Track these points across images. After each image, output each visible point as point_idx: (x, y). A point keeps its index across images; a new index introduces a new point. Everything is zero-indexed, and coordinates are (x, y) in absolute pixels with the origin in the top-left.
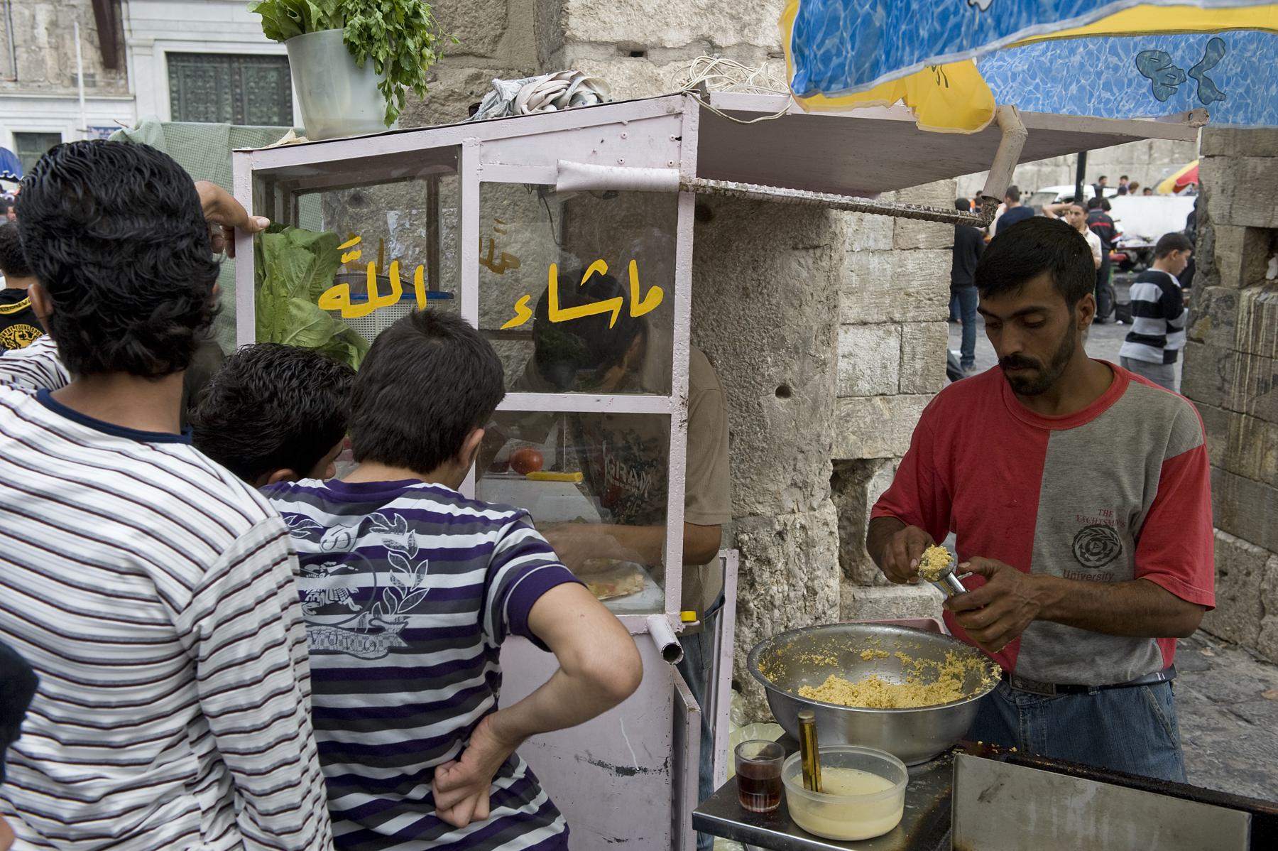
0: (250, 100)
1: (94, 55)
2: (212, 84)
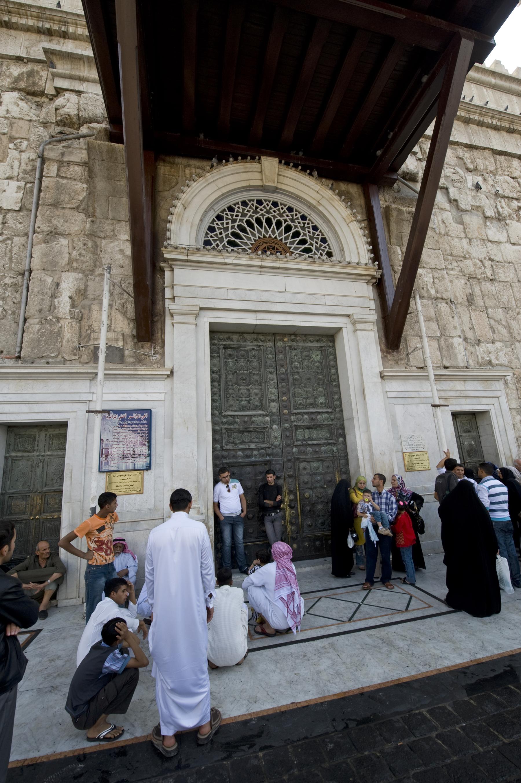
0: (294, 380)
1: (125, 326)
2: (255, 364)
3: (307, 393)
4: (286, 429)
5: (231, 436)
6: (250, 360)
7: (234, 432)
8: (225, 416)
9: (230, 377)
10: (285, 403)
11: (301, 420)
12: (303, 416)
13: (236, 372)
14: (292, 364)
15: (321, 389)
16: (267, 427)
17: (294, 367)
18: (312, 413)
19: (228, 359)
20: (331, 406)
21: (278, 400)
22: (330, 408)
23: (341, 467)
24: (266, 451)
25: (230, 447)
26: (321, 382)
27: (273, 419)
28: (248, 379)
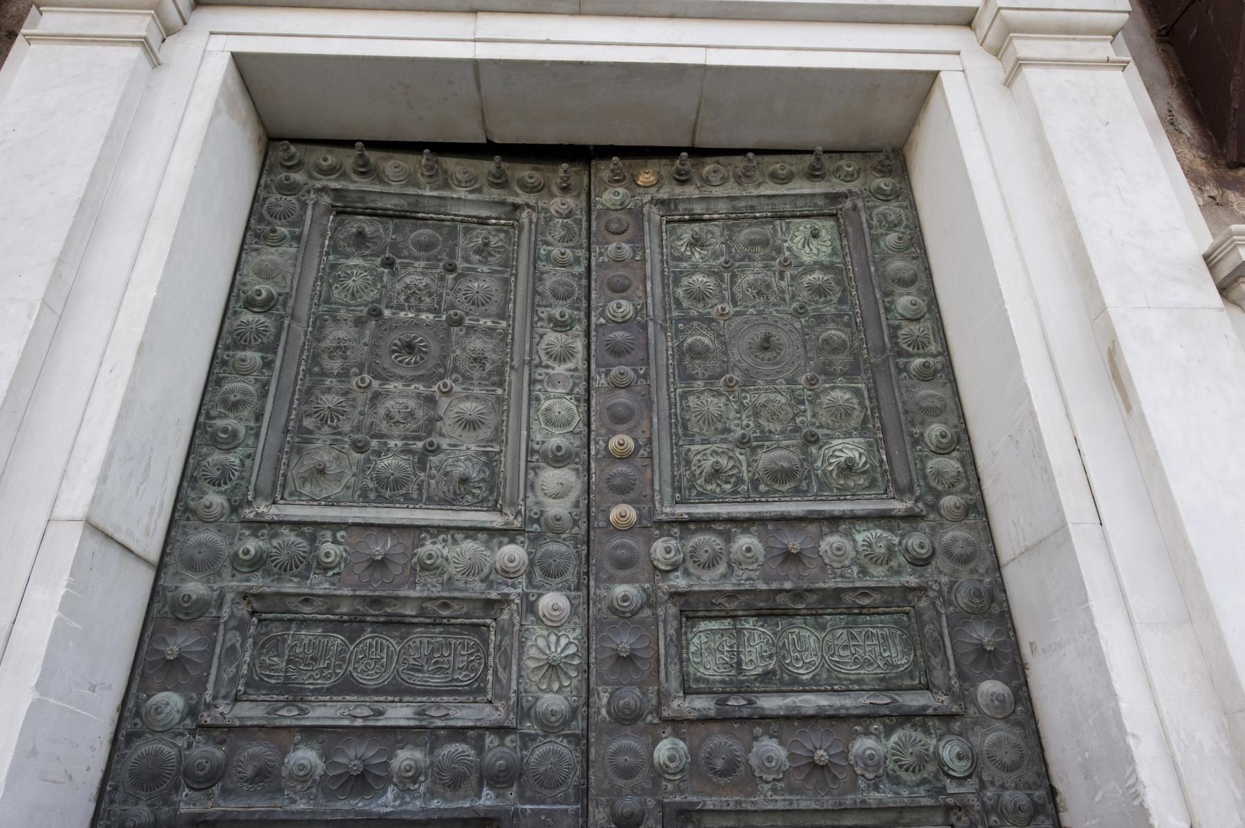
3: (756, 414)
4: (623, 615)
5: (276, 645)
6: (461, 265)
7: (304, 623)
8: (258, 526)
9: (339, 333)
10: (622, 468)
11: (711, 564)
12: (728, 538)
13: (376, 313)
14: (677, 282)
15: (840, 396)
16: (505, 601)
17: (690, 293)
18: (784, 520)
19: (347, 256)
20: (903, 481)
22: (901, 493)
24: (480, 749)
25: (251, 712)
26: (841, 361)
27: (549, 555)
28: (435, 348)
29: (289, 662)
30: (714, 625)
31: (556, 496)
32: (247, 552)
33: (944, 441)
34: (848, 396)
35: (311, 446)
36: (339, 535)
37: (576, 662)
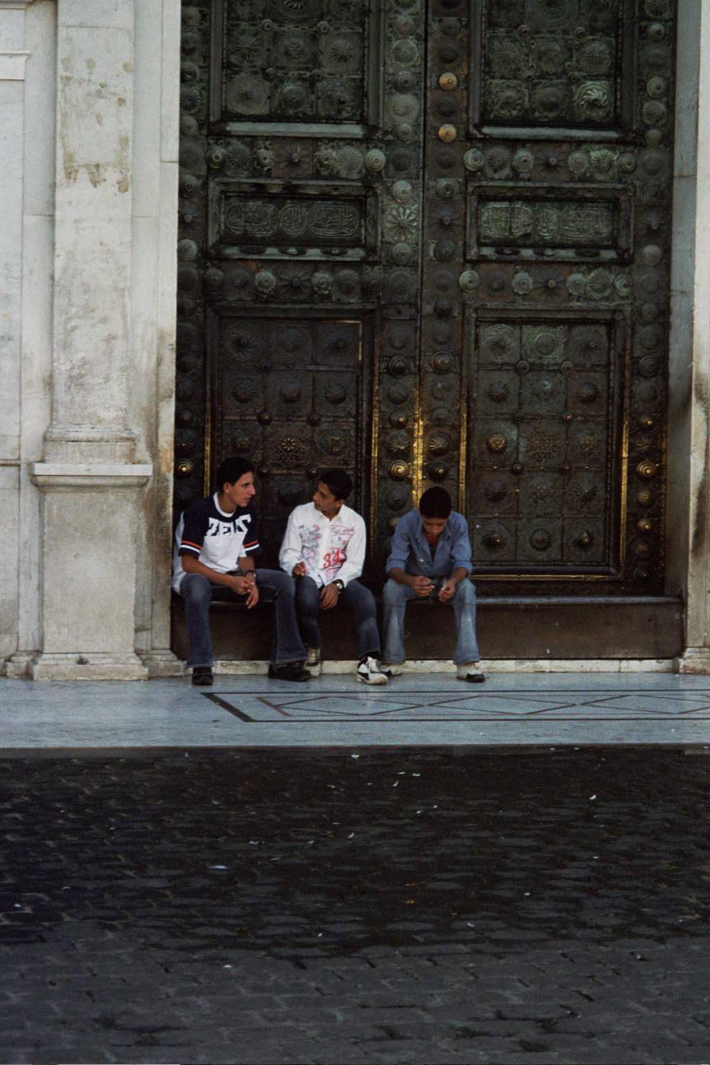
3: (540, 58)
4: (445, 198)
12: (514, 151)
18: (549, 141)
21: (421, 85)
23: (637, 353)
29: (246, 221)
30: (498, 205)
31: (403, 115)
32: (217, 157)
33: (658, 92)
34: (602, 48)
35: (238, 76)
36: (267, 143)
37: (415, 224)
